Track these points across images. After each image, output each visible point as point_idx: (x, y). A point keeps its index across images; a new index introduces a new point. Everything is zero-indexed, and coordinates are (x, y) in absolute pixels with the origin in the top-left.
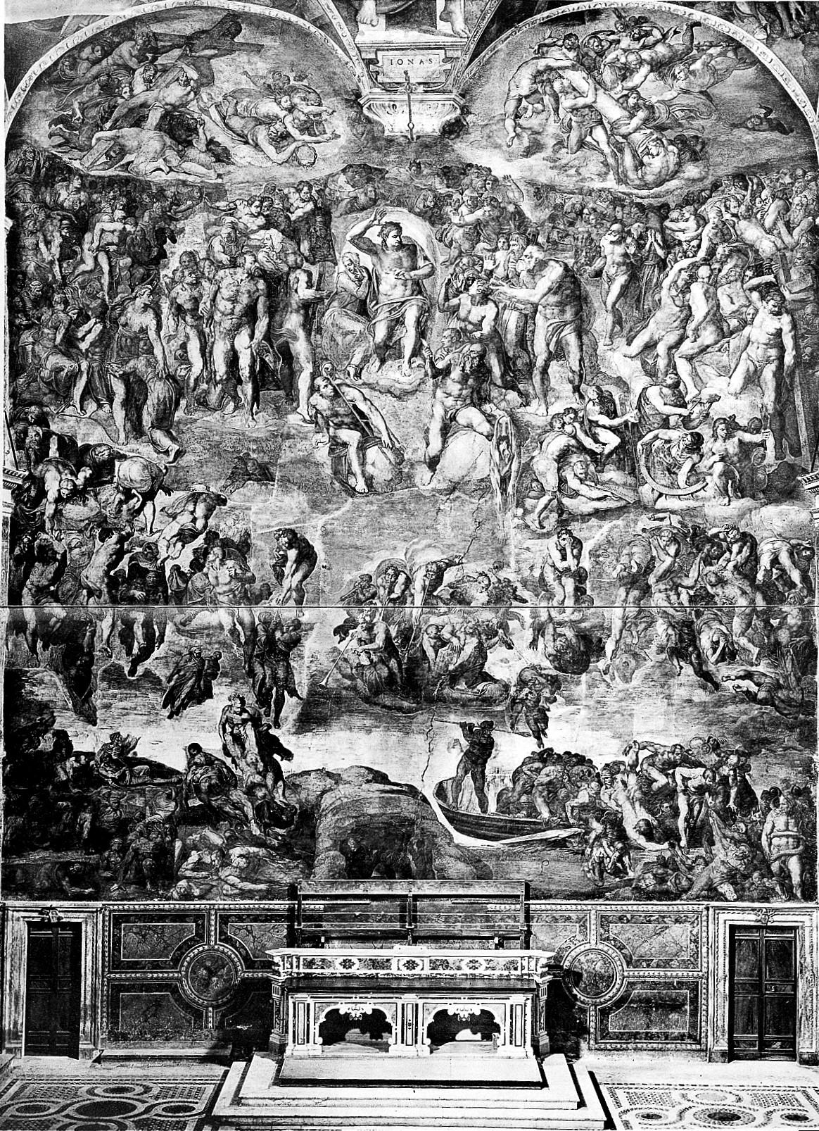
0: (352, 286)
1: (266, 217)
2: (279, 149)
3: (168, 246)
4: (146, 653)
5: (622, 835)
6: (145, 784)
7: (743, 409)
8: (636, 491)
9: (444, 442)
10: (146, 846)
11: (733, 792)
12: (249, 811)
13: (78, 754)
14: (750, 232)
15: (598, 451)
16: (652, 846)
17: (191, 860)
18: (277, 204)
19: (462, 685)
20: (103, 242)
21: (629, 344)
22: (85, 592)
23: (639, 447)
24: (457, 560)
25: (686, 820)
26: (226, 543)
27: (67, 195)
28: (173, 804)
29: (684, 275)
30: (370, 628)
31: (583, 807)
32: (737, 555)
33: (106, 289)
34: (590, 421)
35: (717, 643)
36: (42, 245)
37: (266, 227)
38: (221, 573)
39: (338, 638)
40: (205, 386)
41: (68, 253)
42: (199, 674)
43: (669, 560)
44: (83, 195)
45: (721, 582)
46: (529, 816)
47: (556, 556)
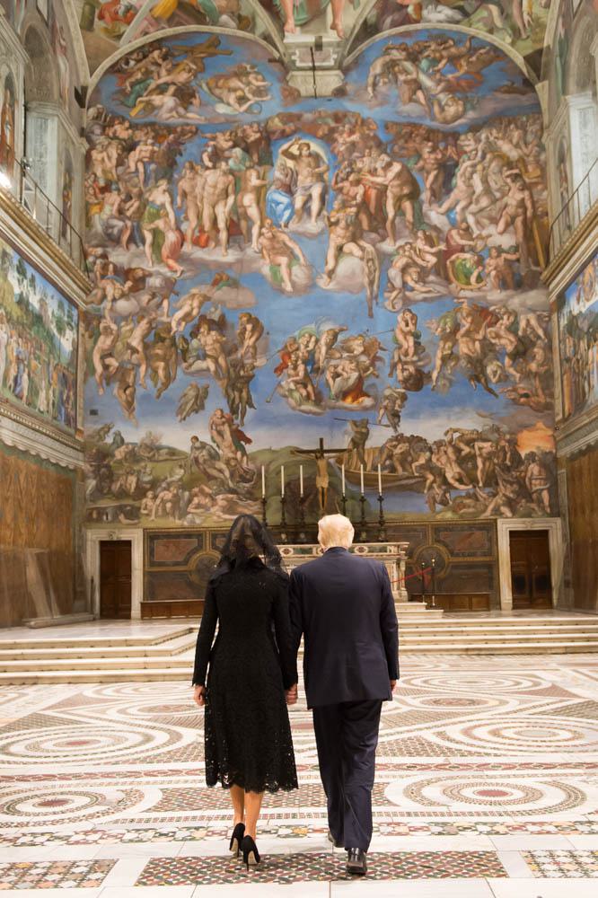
0: (282, 177)
1: (234, 142)
2: (240, 105)
3: (178, 158)
4: (166, 385)
6: (166, 460)
7: (507, 241)
8: (447, 287)
10: (168, 495)
11: (508, 456)
12: (227, 474)
13: (128, 444)
14: (505, 147)
15: (425, 265)
16: (462, 487)
17: (193, 503)
18: (240, 134)
19: (349, 399)
20: (141, 157)
21: (440, 206)
22: (129, 351)
23: (448, 263)
24: (345, 328)
25: (482, 471)
26: (213, 320)
28: (183, 471)
29: (469, 169)
30: (295, 368)
31: (421, 467)
32: (505, 321)
33: (141, 183)
34: (420, 250)
35: (496, 372)
36: (106, 159)
37: (234, 146)
38: (208, 339)
39: (275, 375)
40: (197, 234)
41: (120, 162)
42: (197, 397)
43: (467, 326)
44: (130, 131)
45: (498, 336)
46: (391, 472)
47: (403, 324)
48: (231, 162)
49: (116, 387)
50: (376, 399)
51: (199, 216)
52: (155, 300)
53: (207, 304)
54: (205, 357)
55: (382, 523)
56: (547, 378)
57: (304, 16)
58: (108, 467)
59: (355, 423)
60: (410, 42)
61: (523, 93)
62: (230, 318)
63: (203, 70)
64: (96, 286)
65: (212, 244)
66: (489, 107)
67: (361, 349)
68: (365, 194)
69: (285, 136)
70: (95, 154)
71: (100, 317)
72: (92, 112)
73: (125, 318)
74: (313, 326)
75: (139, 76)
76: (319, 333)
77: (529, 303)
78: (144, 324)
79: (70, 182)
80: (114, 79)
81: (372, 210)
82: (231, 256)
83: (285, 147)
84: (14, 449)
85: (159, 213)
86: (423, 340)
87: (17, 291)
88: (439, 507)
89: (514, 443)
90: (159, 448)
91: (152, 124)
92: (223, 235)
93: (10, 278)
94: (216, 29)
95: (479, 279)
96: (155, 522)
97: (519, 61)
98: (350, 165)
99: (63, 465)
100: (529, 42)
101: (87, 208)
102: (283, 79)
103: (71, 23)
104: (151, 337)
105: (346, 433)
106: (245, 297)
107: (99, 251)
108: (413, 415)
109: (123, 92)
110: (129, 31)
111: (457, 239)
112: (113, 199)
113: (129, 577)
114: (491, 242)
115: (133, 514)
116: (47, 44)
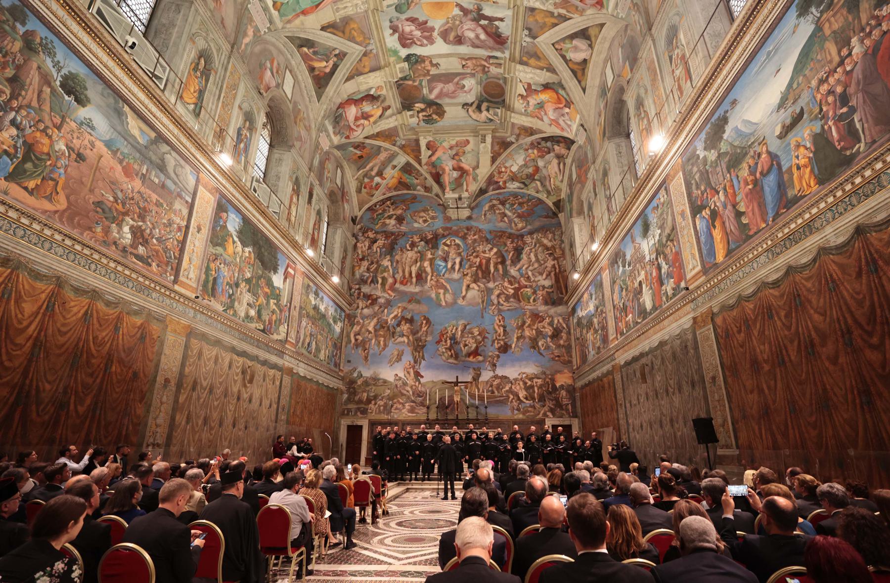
3: (396, 246)
4: (384, 349)
5: (519, 399)
7: (547, 283)
9: (467, 293)
10: (381, 403)
12: (411, 393)
14: (545, 241)
16: (528, 402)
19: (472, 357)
26: (407, 319)
27: (371, 235)
30: (446, 341)
31: (507, 391)
32: (547, 320)
38: (405, 327)
41: (370, 248)
42: (398, 355)
45: (544, 327)
47: (498, 321)
48: (419, 248)
49: (360, 350)
50: (484, 357)
51: (404, 271)
52: (382, 309)
53: (405, 311)
54: (403, 335)
55: (487, 420)
56: (568, 348)
57: (453, 186)
58: (354, 388)
59: (474, 369)
60: (501, 197)
61: (553, 218)
62: (415, 318)
63: (408, 209)
64: (355, 302)
65: (409, 284)
66: (537, 224)
67: (478, 333)
68: (481, 261)
69: (444, 236)
70: (358, 244)
71: (355, 317)
72: (359, 227)
73: (367, 317)
74: (455, 322)
75: (381, 211)
76: (458, 325)
77: (559, 312)
78: (375, 320)
79: (346, 255)
80: (369, 214)
81: (484, 268)
82: (417, 289)
83: (444, 241)
84: (305, 377)
85: (386, 269)
86: (507, 329)
87: (313, 303)
88: (516, 412)
89: (553, 380)
90: (379, 379)
91: (385, 232)
92: (414, 280)
93: (310, 297)
94: (415, 192)
95: (534, 300)
96: (374, 416)
97: (551, 204)
98: (473, 249)
99: (331, 386)
100: (555, 197)
101: (353, 267)
102: (444, 212)
103: (352, 191)
104: (378, 327)
105: (469, 373)
106: (423, 308)
107: (357, 286)
108: (503, 365)
109: (373, 218)
110: (377, 193)
111: (523, 282)
112: (365, 264)
113: (360, 444)
114: (539, 284)
115: (364, 412)
116: (339, 198)
